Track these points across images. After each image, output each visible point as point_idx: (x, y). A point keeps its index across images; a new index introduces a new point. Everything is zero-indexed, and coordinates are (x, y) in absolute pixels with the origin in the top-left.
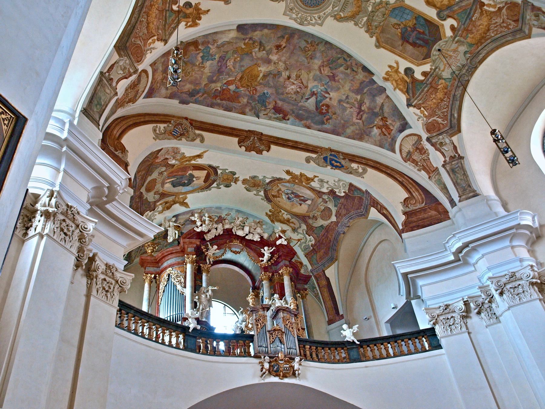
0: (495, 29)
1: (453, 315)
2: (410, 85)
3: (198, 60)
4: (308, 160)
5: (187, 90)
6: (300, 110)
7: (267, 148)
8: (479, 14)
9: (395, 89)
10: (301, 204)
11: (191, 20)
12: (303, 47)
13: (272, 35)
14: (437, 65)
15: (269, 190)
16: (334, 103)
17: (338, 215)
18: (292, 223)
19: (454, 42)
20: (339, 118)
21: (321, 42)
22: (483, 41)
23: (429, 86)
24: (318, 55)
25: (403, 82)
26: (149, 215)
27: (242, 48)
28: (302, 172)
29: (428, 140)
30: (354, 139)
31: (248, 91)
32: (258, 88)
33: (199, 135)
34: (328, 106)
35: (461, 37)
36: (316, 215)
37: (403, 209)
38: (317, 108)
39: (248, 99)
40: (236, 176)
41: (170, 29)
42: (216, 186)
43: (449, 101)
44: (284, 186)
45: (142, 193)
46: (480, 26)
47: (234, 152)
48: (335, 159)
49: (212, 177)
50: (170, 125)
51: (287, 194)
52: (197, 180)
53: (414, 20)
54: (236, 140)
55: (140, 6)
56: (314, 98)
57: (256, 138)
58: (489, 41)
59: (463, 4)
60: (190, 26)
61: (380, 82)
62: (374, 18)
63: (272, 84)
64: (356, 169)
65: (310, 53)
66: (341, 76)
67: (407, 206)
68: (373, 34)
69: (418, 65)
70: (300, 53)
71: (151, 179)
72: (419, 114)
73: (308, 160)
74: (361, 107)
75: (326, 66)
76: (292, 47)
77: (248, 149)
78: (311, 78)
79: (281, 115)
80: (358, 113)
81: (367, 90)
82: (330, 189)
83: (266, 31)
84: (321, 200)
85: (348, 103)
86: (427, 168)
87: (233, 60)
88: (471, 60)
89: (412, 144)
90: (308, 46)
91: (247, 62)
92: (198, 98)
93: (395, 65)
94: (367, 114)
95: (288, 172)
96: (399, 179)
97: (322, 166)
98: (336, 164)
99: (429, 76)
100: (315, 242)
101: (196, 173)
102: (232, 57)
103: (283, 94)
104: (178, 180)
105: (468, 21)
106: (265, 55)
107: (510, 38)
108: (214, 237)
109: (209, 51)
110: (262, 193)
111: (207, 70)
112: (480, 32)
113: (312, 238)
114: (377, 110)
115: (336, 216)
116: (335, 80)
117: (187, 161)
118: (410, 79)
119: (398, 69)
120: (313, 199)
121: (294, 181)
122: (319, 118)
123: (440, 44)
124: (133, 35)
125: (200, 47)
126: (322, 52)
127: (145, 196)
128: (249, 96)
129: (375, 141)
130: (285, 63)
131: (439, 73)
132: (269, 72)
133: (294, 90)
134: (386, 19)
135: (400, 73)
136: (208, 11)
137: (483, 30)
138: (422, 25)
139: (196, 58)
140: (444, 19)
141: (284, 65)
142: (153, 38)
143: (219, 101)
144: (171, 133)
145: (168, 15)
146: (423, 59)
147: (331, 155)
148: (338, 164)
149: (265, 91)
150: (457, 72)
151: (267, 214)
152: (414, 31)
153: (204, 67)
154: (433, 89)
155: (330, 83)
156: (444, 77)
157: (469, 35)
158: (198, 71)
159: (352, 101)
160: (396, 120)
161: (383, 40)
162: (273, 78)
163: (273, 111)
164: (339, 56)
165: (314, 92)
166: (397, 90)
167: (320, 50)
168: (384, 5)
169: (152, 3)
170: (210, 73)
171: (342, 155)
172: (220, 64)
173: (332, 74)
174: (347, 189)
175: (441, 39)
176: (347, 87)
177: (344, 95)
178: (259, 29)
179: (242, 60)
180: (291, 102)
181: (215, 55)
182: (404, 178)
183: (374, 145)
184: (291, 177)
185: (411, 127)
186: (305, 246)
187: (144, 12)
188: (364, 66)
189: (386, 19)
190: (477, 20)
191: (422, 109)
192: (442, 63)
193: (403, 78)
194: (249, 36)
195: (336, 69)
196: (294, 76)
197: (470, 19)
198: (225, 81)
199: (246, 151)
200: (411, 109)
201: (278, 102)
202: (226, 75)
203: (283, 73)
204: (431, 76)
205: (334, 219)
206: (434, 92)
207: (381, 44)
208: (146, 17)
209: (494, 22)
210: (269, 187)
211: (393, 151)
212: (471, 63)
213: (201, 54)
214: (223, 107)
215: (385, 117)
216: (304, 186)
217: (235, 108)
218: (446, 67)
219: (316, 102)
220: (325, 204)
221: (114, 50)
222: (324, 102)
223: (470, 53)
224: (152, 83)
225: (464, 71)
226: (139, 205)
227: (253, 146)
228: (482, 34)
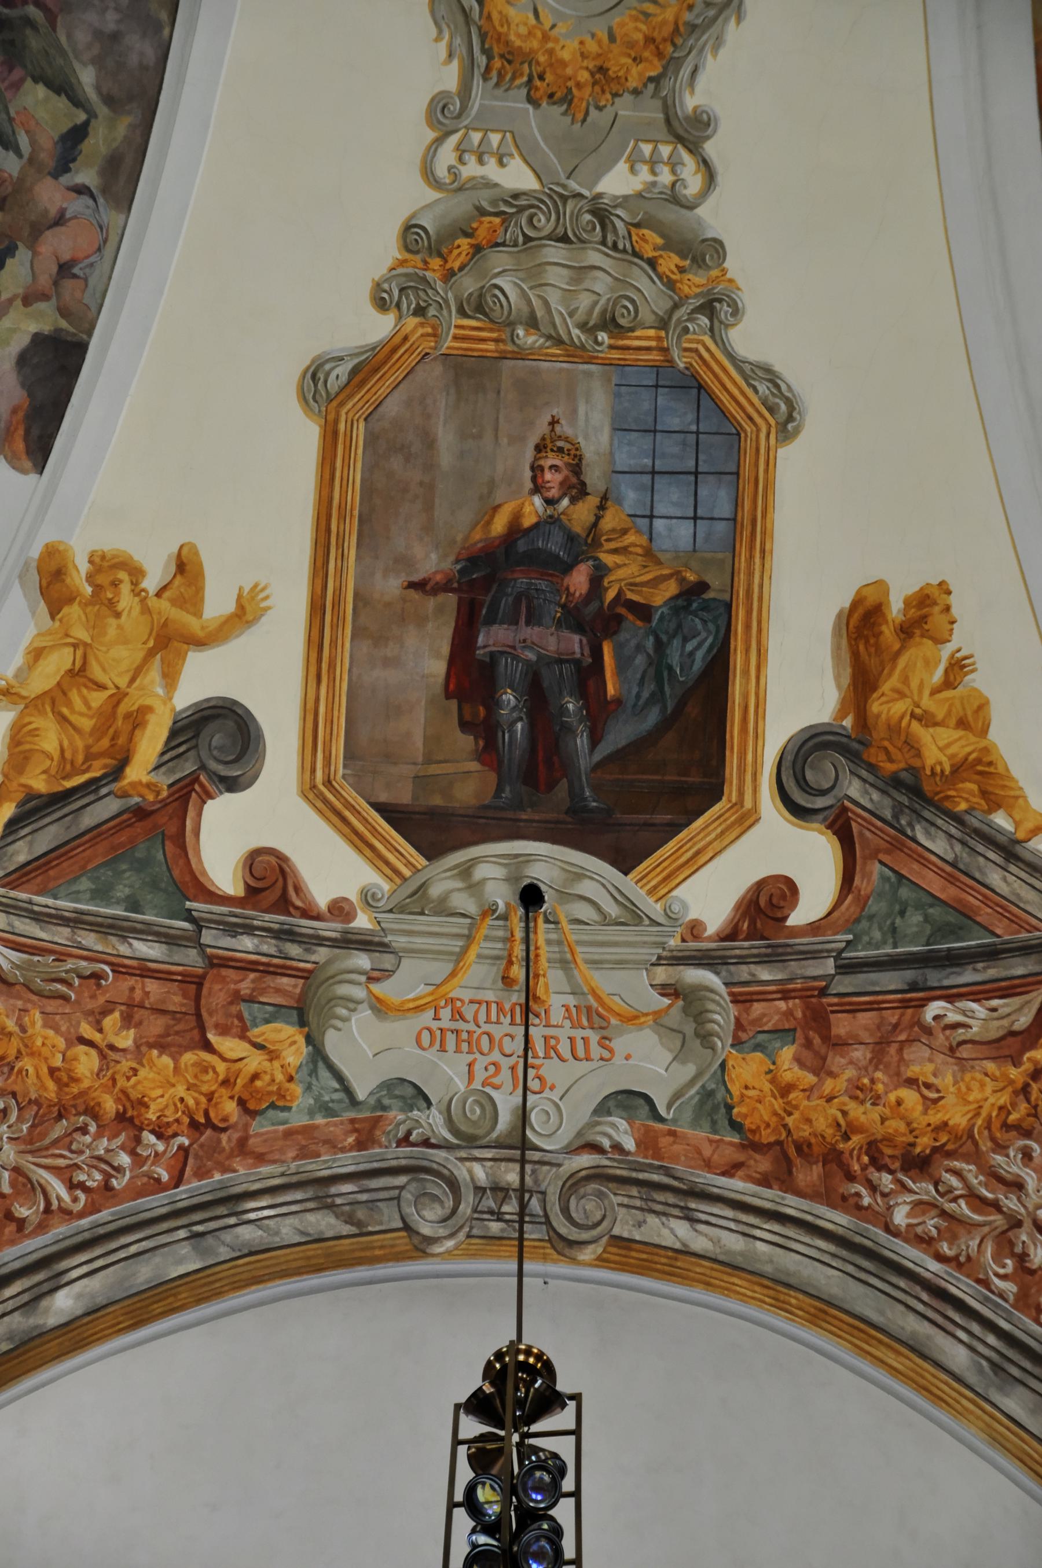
0: (963, 1208)
2: (106, 808)
8: (996, 1029)
14: (399, 941)
19: (662, 974)
22: (808, 1175)
23: (190, 958)
25: (99, 732)
35: (736, 999)
43: (157, 1186)
46: (911, 1082)
53: (671, 588)
58: (837, 1219)
59: (995, 878)
62: (555, 253)
68: (409, 303)
88: (597, 1175)
99: (274, 919)
105: (891, 980)
107: (958, 1356)
112: (863, 1114)
118: (163, 780)
119: (200, 643)
123: (579, 875)
131: (343, 990)
134: (576, 353)
135: (171, 678)
137: (895, 1125)
138: (659, 665)
140: (800, 798)
146: (388, 812)
150: (434, 1122)
152: (579, 627)
154: (176, 1001)
156: (332, 1042)
157: (787, 1053)
161: (392, 408)
164: (87, 77)
168: (695, 282)
175: (625, 862)
188: (81, 349)
189: (576, 353)
190: (941, 1039)
192: (440, 969)
193: (138, 720)
197: (913, 987)
206: (156, 1026)
207: (354, 407)
209: (1009, 1164)
212: (575, 1184)
218: (426, 1018)
223: (647, 1142)
225: (480, 1173)
228: (856, 1139)
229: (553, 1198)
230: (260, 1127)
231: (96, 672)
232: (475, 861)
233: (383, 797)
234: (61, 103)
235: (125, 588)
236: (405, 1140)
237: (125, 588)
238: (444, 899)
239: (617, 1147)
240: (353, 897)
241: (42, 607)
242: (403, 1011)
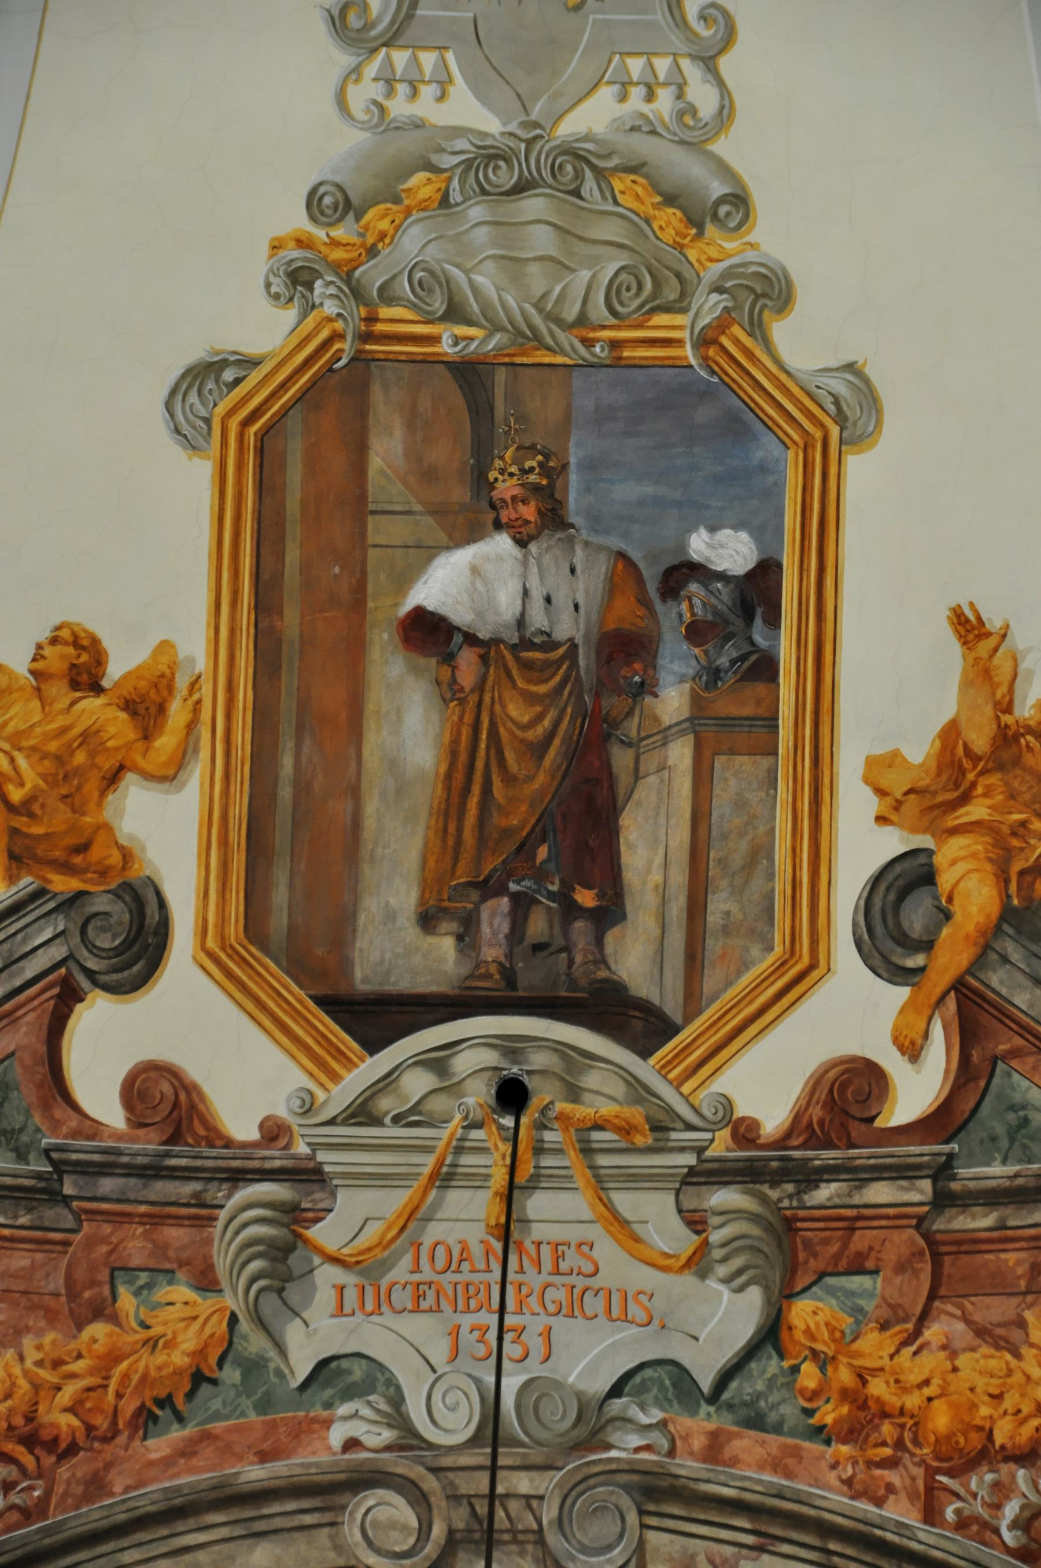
169: (829, 1414)
187: (931, 1515)
208: (981, 1480)
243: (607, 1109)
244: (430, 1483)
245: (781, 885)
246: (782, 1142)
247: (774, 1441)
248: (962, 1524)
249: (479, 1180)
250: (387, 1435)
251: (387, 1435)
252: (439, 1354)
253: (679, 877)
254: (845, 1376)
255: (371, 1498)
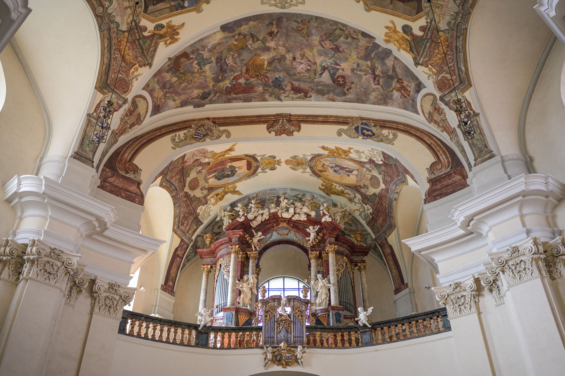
1: (464, 294)
2: (412, 43)
3: (195, 68)
4: (339, 134)
5: (196, 95)
6: (318, 86)
7: (298, 128)
9: (399, 50)
10: (348, 175)
11: (168, 38)
12: (295, 27)
13: (260, 25)
15: (314, 166)
16: (348, 73)
17: (385, 182)
18: (347, 194)
20: (358, 87)
21: (312, 19)
24: (314, 31)
25: (404, 41)
26: (203, 209)
27: (235, 44)
28: (337, 146)
29: (441, 99)
30: (380, 105)
31: (260, 80)
32: (268, 75)
33: (224, 131)
34: (343, 77)
36: (366, 184)
37: (428, 176)
38: (334, 81)
39: (263, 87)
40: (277, 159)
41: (150, 53)
42: (261, 171)
44: (326, 160)
45: (187, 193)
47: (265, 139)
48: (367, 127)
49: (254, 164)
50: (191, 130)
51: (332, 167)
52: (239, 169)
54: (264, 126)
55: (107, 46)
56: (326, 72)
57: (285, 120)
60: (170, 43)
61: (384, 45)
63: (281, 68)
64: (387, 136)
65: (305, 31)
66: (344, 46)
67: (432, 173)
69: (414, 21)
70: (295, 34)
71: (190, 179)
72: (429, 72)
73: (339, 134)
74: (374, 72)
75: (326, 40)
76: (285, 31)
77: (278, 133)
78: (316, 54)
79: (302, 94)
80: (375, 79)
81: (375, 55)
82: (369, 158)
83: (251, 23)
84: (365, 169)
85: (361, 71)
86: (447, 129)
87: (231, 58)
88: (462, 6)
89: (430, 105)
90: (300, 25)
91: (246, 56)
92: (211, 98)
93: (391, 25)
94: (382, 78)
95: (323, 148)
96: (428, 141)
97: (354, 138)
98: (367, 133)
99: (427, 30)
100: (373, 211)
101: (235, 164)
102: (228, 55)
103: (295, 75)
104: (220, 174)
106: (261, 45)
108: (260, 223)
109: (203, 57)
110: (308, 170)
111: (208, 73)
113: (370, 207)
114: (390, 73)
115: (384, 183)
116: (339, 51)
117: (220, 156)
118: (410, 36)
119: (395, 28)
120: (358, 169)
121: (334, 155)
122: (338, 90)
124: (111, 72)
125: (191, 56)
126: (316, 27)
127: (192, 194)
128: (263, 84)
129: (399, 104)
130: (284, 46)
132: (273, 59)
133: (305, 69)
135: (399, 32)
136: (183, 24)
139: (192, 66)
141: (284, 48)
142: (134, 67)
143: (235, 96)
144: (193, 137)
145: (141, 43)
147: (362, 124)
148: (370, 133)
149: (277, 76)
150: (453, 22)
151: (320, 188)
153: (204, 72)
154: (434, 44)
155: (336, 55)
158: (200, 76)
159: (364, 68)
160: (411, 81)
161: (371, 2)
162: (279, 63)
163: (292, 92)
164: (334, 27)
165: (324, 66)
166: (401, 50)
167: (313, 26)
169: (119, 39)
170: (213, 74)
171: (373, 122)
172: (219, 65)
173: (335, 46)
174: (382, 157)
176: (354, 55)
177: (354, 63)
178: (244, 23)
179: (240, 55)
180: (306, 80)
181: (210, 58)
182: (433, 140)
183: (400, 108)
184: (328, 151)
185: (425, 87)
186: (364, 215)
187: (114, 50)
191: (430, 66)
193: (403, 37)
194: (237, 32)
195: (336, 40)
196: (298, 55)
198: (232, 77)
199: (276, 135)
200: (420, 67)
201: (294, 82)
202: (230, 72)
203: (287, 56)
204: (429, 29)
205: (382, 186)
206: (436, 47)
207: (370, 6)
208: (118, 52)
210: (313, 164)
211: (418, 114)
212: (463, 9)
213: (196, 62)
214: (241, 100)
215: (400, 79)
216: (345, 159)
217: (254, 98)
218: (441, 18)
219: (331, 75)
220: (370, 173)
221: (96, 91)
222: (338, 74)
224: (153, 101)
226: (189, 202)
227: (282, 129)
229: (464, 12)
230: (449, 41)
231: (397, 39)
232: (424, 6)
233: (415, 14)
234: (337, 30)
235: (389, 34)
236: (454, 26)
237: (389, 34)
238: (428, 11)
239: (460, 3)
240: (426, 21)
241: (390, 43)
242: (440, 20)
243: (138, 11)
244: (104, 12)
245: (160, 17)
246: (139, 26)
247: (116, 36)
248: (114, 53)
249: (129, 4)
250: (107, 7)
251: (107, 7)
252: (114, 8)
253: (158, 9)
254: (122, 39)
255: (102, 8)
